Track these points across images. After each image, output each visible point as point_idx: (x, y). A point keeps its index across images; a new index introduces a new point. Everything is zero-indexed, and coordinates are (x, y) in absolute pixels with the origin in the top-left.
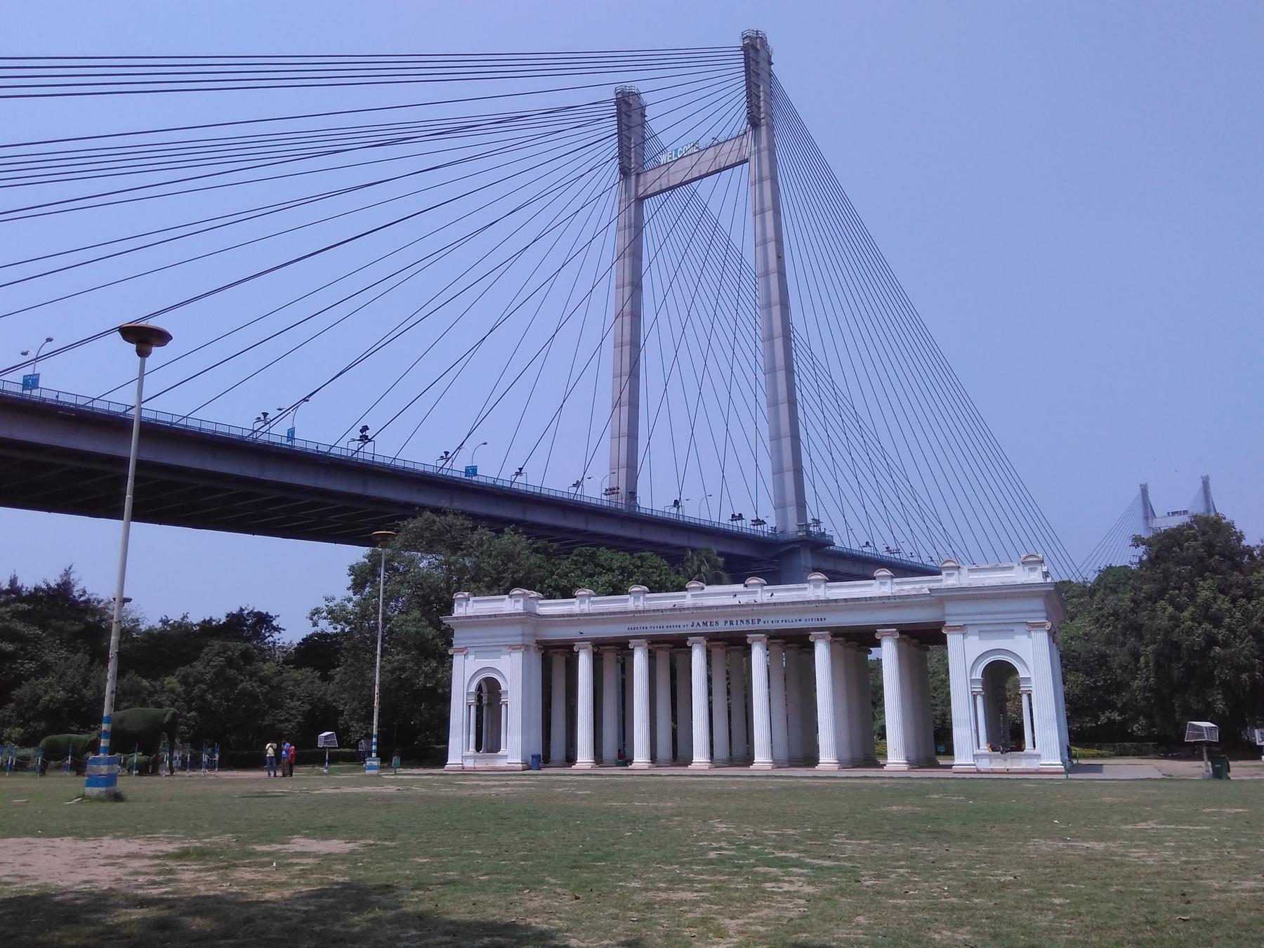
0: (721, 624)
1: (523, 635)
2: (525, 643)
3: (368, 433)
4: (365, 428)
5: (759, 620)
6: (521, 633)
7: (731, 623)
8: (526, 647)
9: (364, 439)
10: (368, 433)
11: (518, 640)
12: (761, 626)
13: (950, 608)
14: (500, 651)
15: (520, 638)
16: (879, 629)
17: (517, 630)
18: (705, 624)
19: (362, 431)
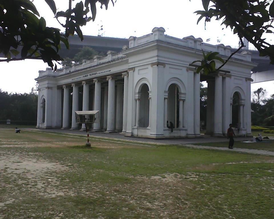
0: (89, 75)
1: (48, 83)
2: (49, 86)
3: (102, 27)
4: (102, 26)
5: (96, 73)
6: (47, 83)
7: (91, 75)
8: (48, 88)
9: (102, 29)
10: (102, 27)
11: (46, 86)
12: (97, 75)
13: (131, 59)
14: (44, 89)
15: (47, 85)
16: (123, 73)
17: (46, 82)
18: (86, 76)
19: (101, 27)
